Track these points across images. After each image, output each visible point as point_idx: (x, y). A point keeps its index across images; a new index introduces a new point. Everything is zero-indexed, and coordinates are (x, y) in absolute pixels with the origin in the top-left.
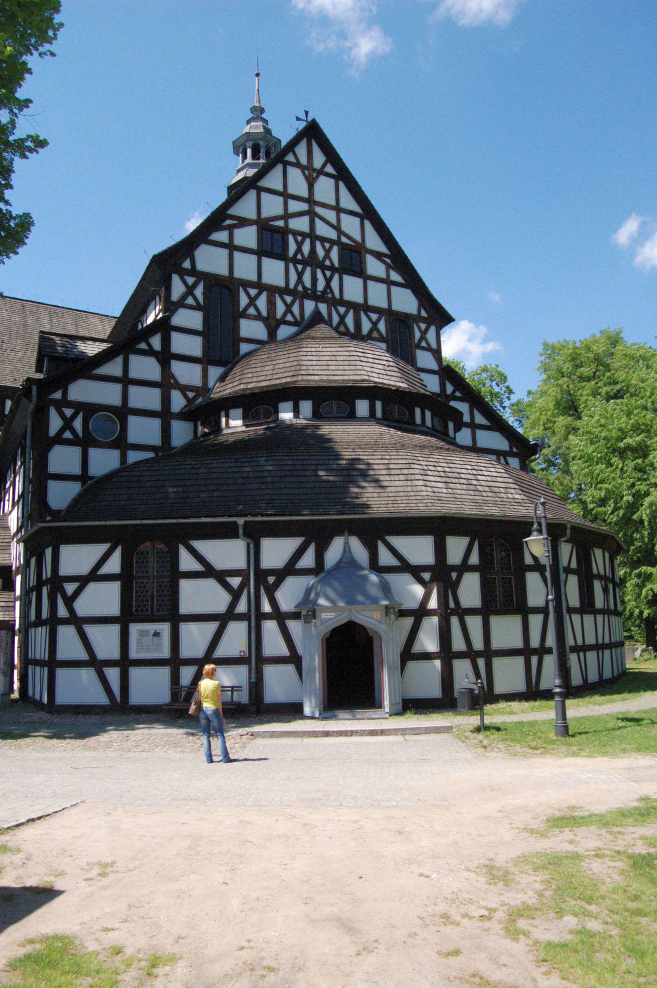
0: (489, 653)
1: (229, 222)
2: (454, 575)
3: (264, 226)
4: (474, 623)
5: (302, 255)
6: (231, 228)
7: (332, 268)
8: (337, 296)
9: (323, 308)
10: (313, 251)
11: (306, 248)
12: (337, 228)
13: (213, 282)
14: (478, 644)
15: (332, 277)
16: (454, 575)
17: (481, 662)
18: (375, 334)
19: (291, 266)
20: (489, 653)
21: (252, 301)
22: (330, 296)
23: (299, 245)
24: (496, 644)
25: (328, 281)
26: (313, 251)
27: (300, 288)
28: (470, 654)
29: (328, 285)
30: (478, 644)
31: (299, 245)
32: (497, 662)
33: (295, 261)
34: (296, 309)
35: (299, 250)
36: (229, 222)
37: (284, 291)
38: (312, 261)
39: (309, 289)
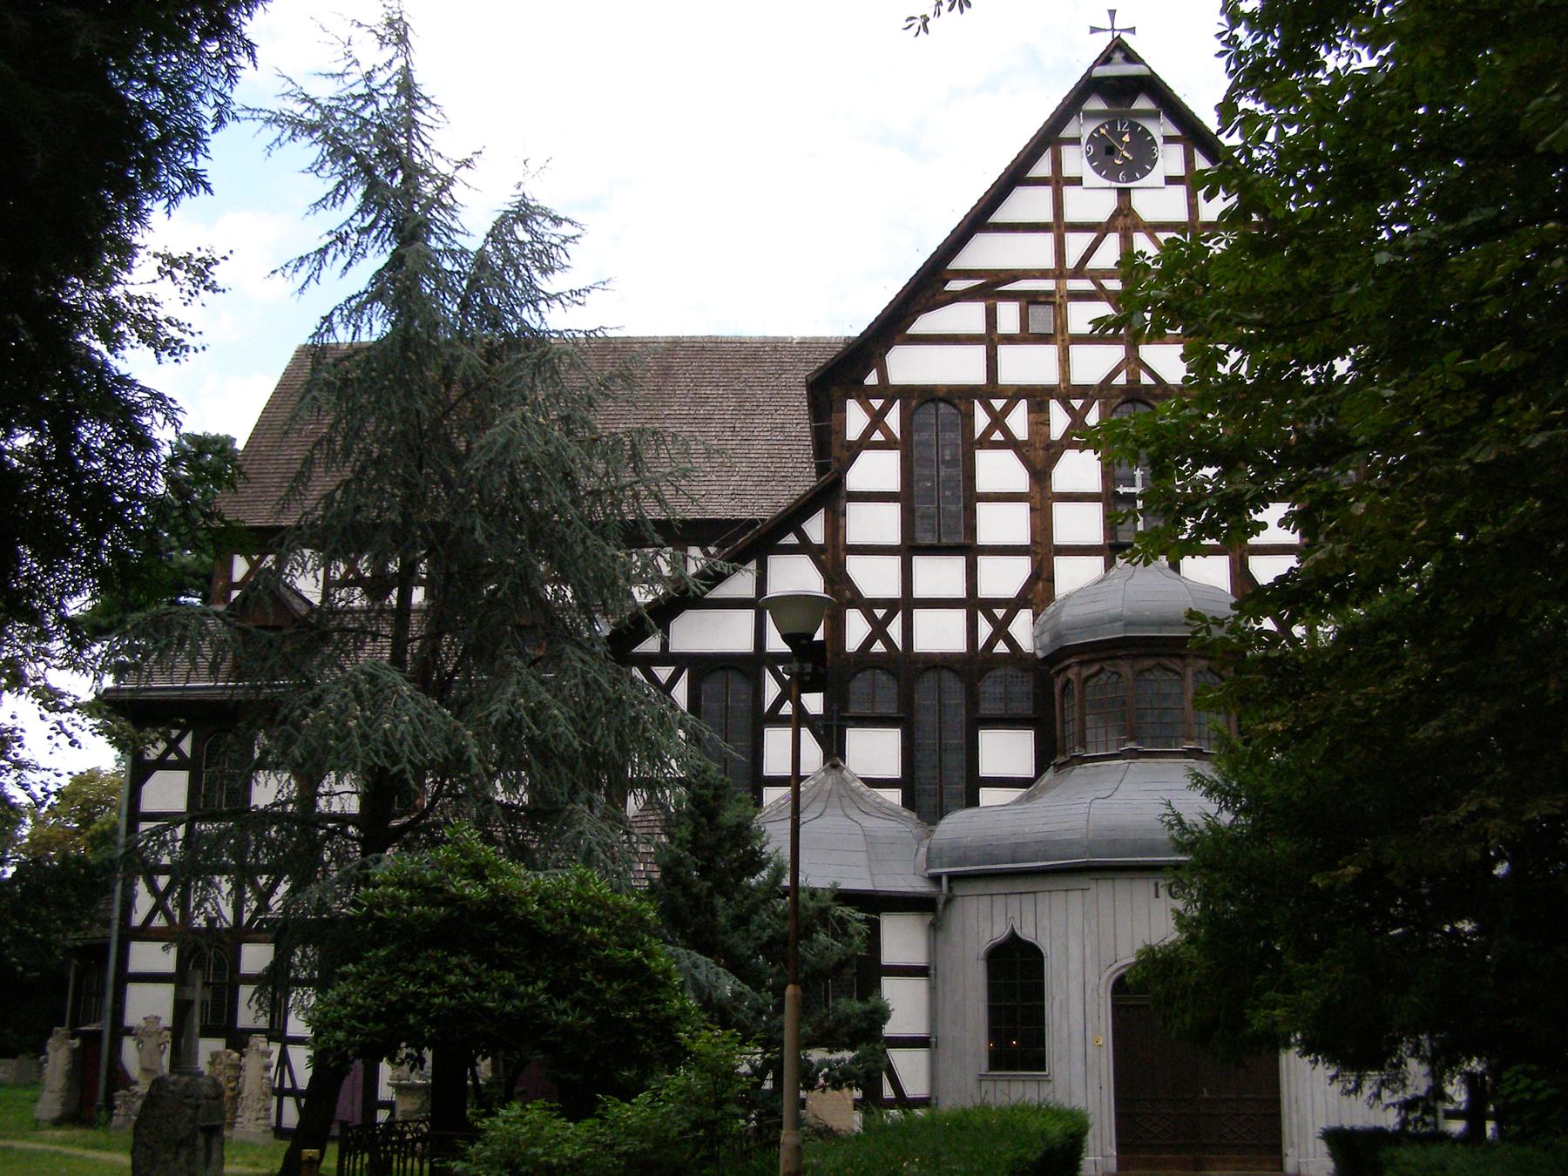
13: (919, 398)
21: (998, 420)
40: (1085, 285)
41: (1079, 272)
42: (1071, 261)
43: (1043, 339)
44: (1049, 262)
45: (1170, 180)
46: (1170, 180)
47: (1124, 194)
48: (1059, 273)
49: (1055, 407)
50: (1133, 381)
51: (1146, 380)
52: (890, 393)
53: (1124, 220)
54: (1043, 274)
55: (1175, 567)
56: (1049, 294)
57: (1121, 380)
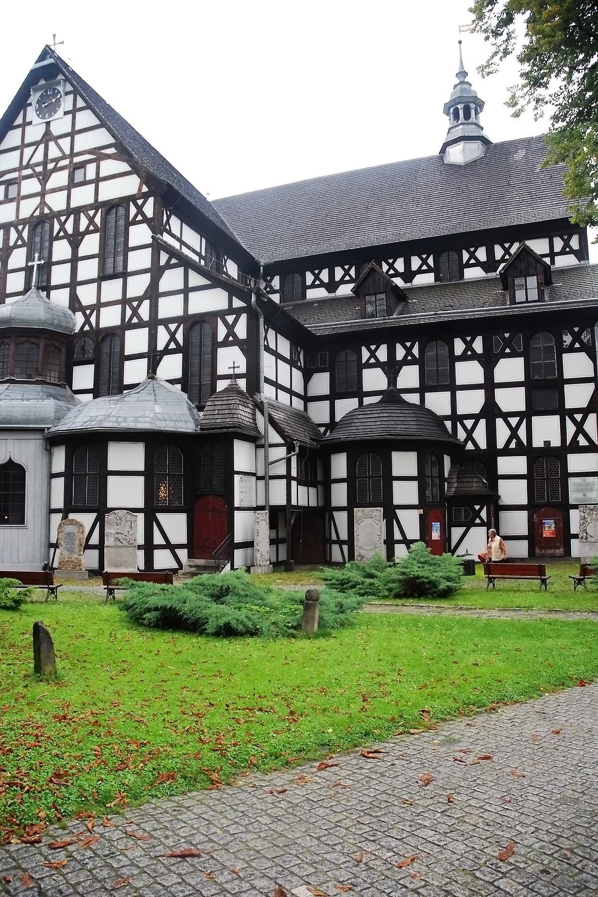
40: (29, 172)
41: (27, 167)
42: (25, 163)
43: (12, 200)
44: (17, 165)
45: (66, 113)
46: (66, 113)
47: (48, 124)
48: (21, 168)
49: (12, 230)
50: (42, 212)
51: (46, 211)
53: (48, 137)
54: (14, 170)
55: (48, 296)
56: (16, 179)
57: (37, 213)
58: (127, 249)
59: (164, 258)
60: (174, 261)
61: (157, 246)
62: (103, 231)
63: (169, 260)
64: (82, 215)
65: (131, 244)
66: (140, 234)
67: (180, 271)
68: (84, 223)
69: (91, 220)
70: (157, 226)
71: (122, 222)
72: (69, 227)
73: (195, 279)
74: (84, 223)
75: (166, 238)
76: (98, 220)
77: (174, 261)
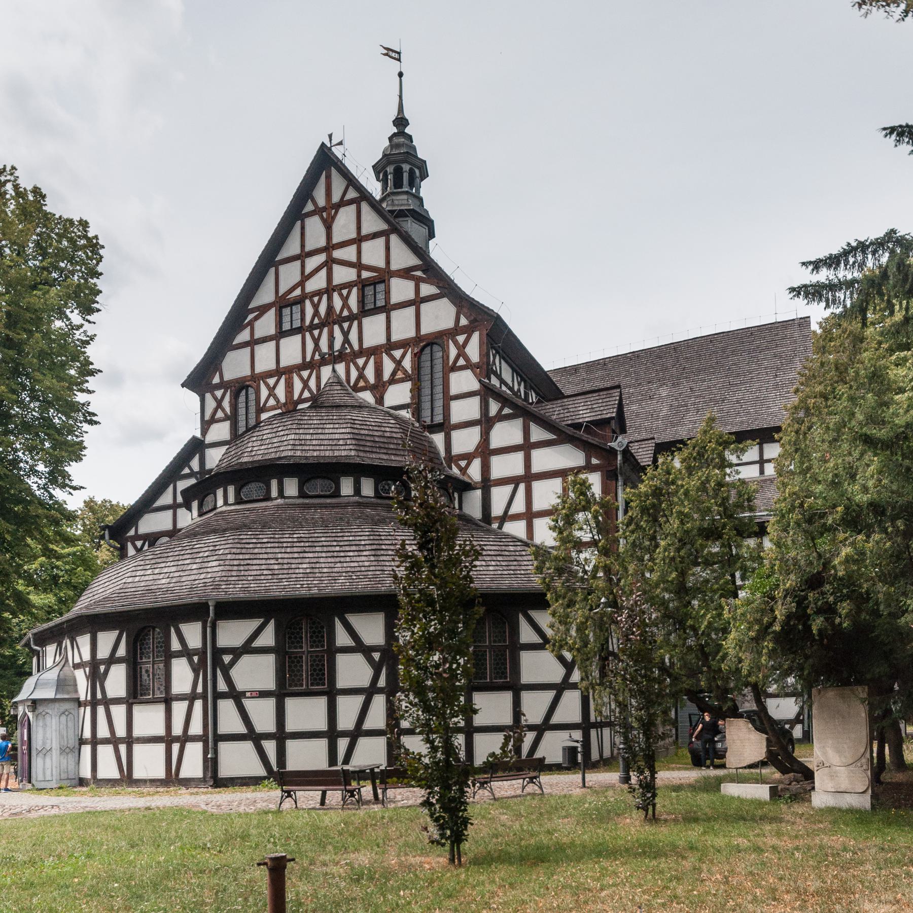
0: (130, 741)
1: (251, 317)
2: (102, 668)
3: (282, 303)
4: (119, 712)
5: (319, 318)
6: (251, 324)
7: (351, 318)
8: (356, 347)
9: (341, 368)
10: (330, 308)
11: (323, 309)
12: (359, 266)
14: (121, 732)
15: (350, 327)
16: (102, 668)
17: (123, 748)
18: (400, 375)
19: (308, 335)
20: (130, 741)
21: (272, 390)
22: (348, 351)
23: (316, 307)
24: (137, 733)
25: (346, 334)
26: (330, 308)
27: (317, 357)
28: (113, 741)
29: (346, 341)
30: (121, 732)
31: (316, 307)
32: (137, 748)
33: (312, 327)
34: (312, 383)
35: (316, 313)
36: (251, 317)
37: (304, 366)
38: (331, 319)
39: (326, 354)
52: (223, 385)
58: (448, 398)
59: (494, 408)
60: (507, 411)
61: (486, 393)
62: (416, 378)
63: (501, 410)
64: (386, 360)
65: (454, 391)
66: (463, 381)
67: (518, 423)
68: (388, 366)
69: (398, 363)
70: (484, 370)
71: (438, 367)
72: (370, 373)
73: (538, 434)
74: (388, 366)
75: (495, 381)
76: (407, 364)
77: (507, 411)
